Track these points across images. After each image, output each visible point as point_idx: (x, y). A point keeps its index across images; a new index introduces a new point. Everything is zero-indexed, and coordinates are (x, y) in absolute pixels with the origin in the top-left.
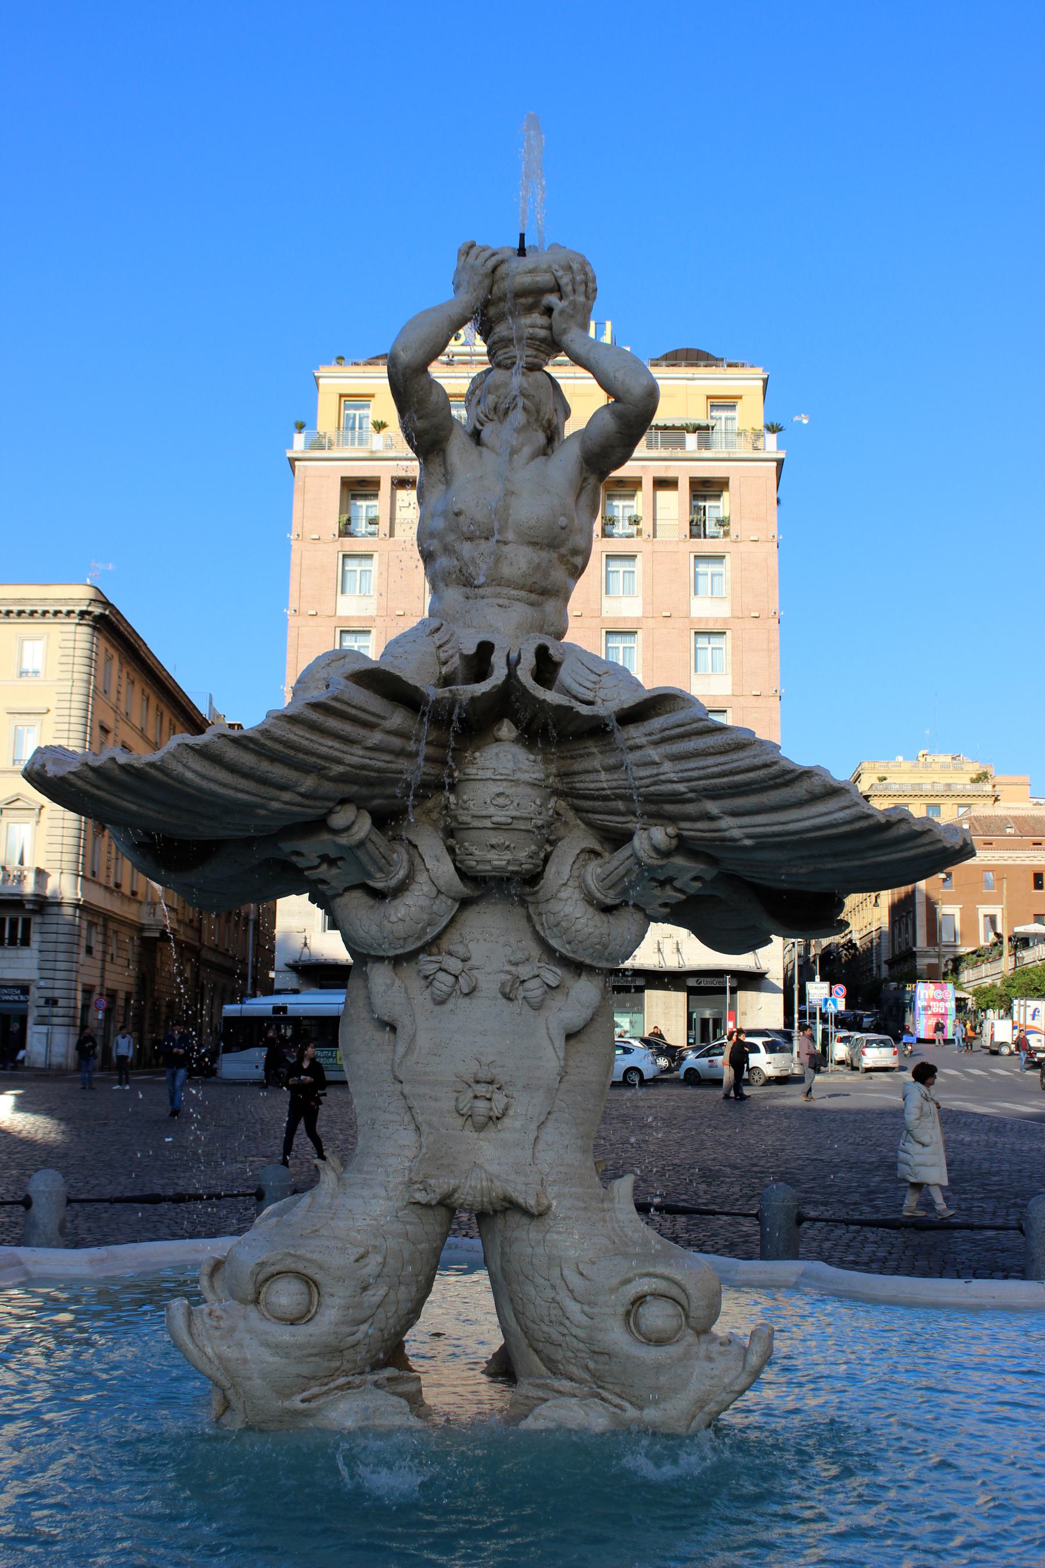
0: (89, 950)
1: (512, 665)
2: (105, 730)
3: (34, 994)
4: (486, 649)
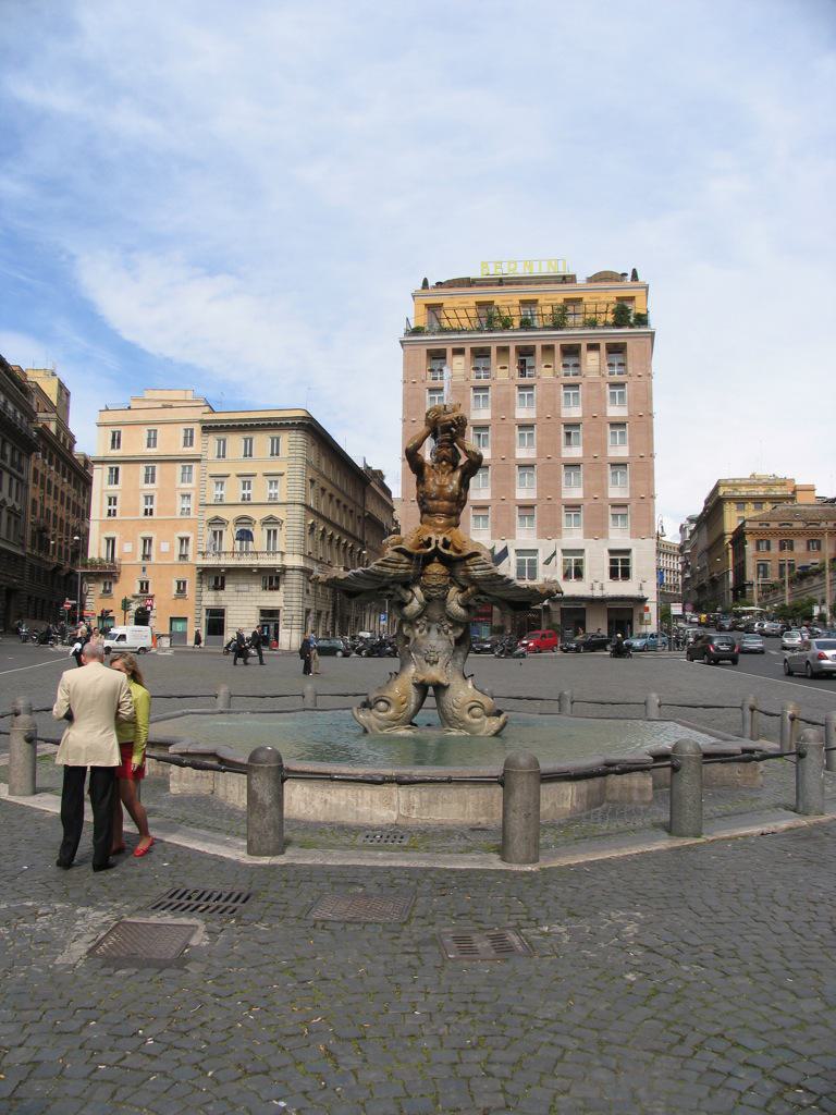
0: (308, 591)
1: (437, 542)
2: (312, 481)
3: (282, 614)
4: (430, 539)
